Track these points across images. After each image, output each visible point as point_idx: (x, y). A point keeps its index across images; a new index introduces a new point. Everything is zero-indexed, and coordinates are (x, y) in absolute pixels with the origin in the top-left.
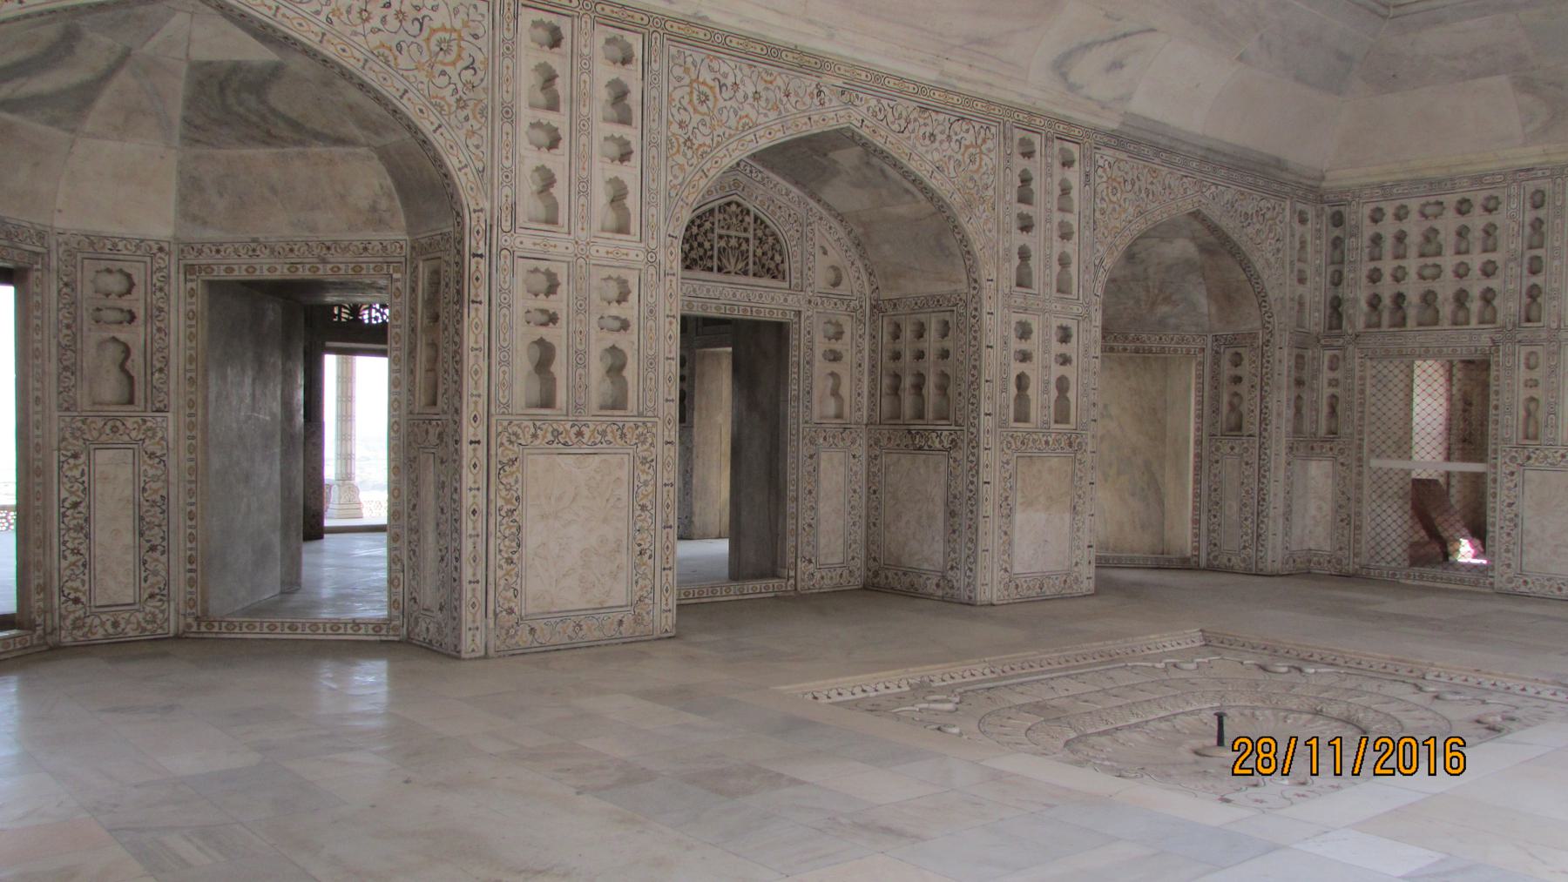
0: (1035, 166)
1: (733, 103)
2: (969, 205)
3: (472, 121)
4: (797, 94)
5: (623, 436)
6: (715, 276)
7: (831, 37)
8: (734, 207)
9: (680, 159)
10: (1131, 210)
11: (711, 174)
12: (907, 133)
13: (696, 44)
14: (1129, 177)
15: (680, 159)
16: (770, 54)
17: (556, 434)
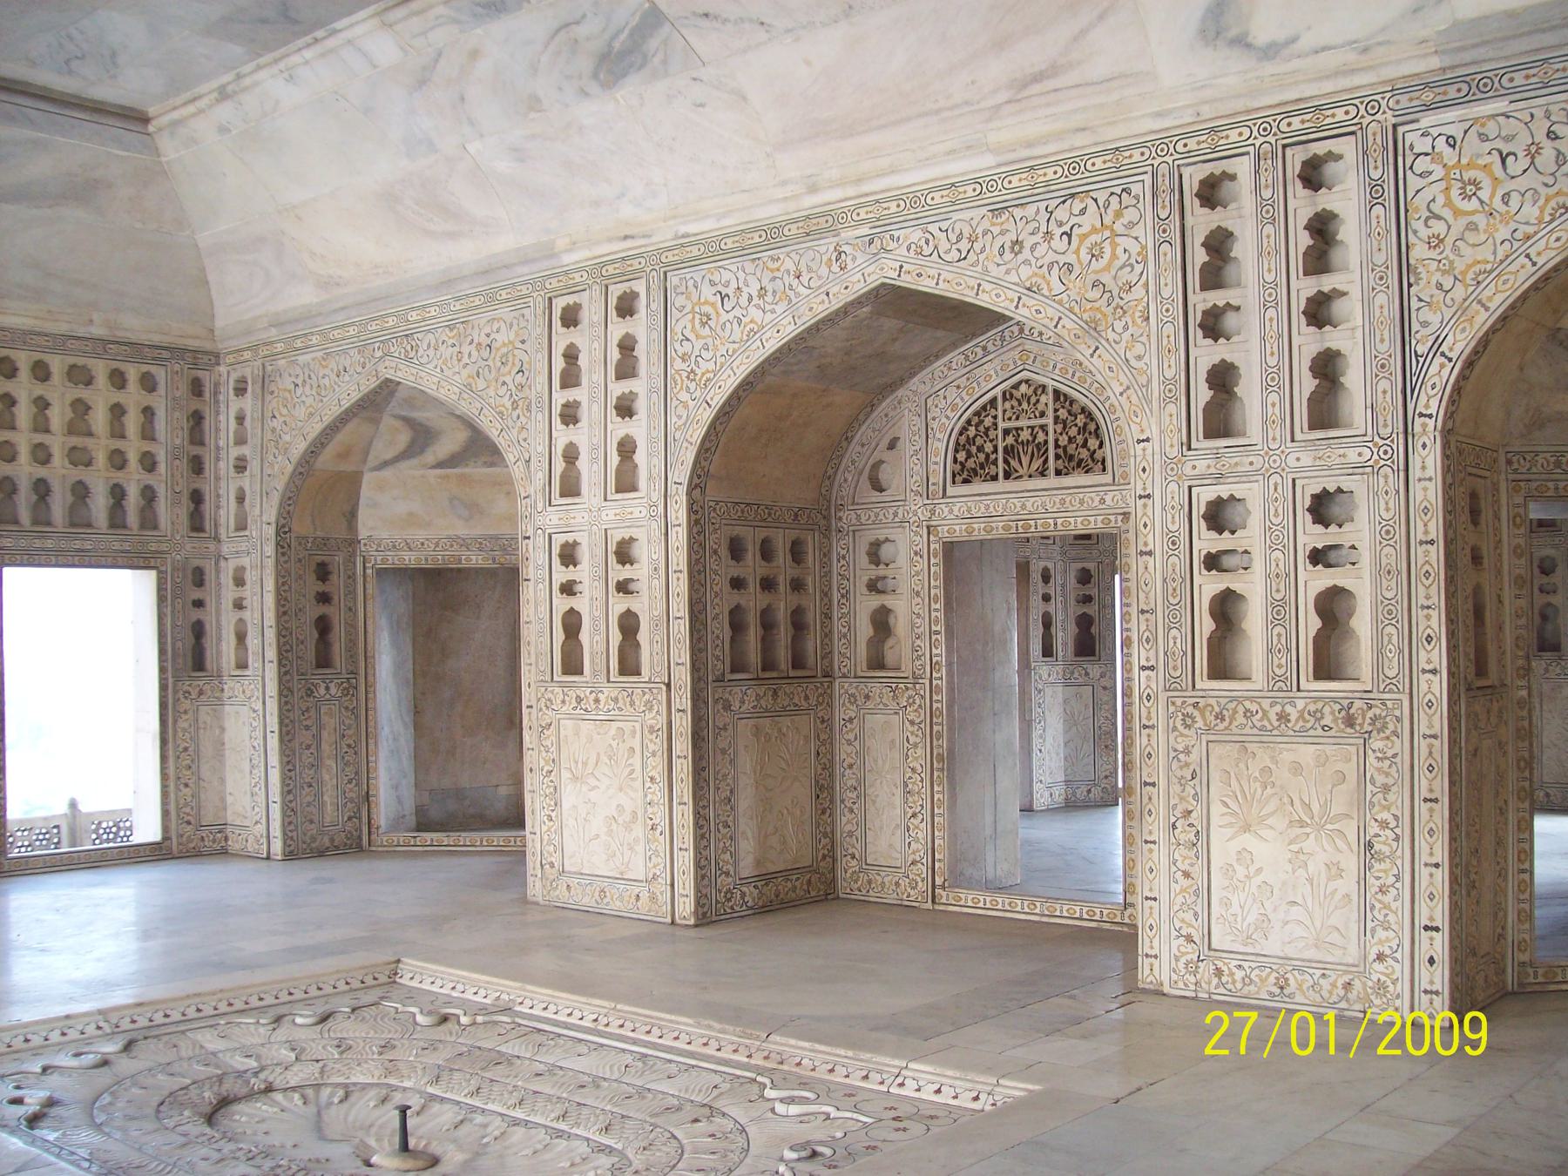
0: (1242, 217)
1: (737, 312)
2: (1093, 327)
3: (522, 418)
4: (810, 270)
5: (632, 704)
6: (1002, 485)
7: (813, 189)
8: (1023, 388)
9: (684, 396)
10: (1531, 212)
11: (713, 404)
12: (972, 257)
13: (693, 263)
14: (1519, 147)
15: (684, 396)
16: (772, 236)
17: (579, 700)
